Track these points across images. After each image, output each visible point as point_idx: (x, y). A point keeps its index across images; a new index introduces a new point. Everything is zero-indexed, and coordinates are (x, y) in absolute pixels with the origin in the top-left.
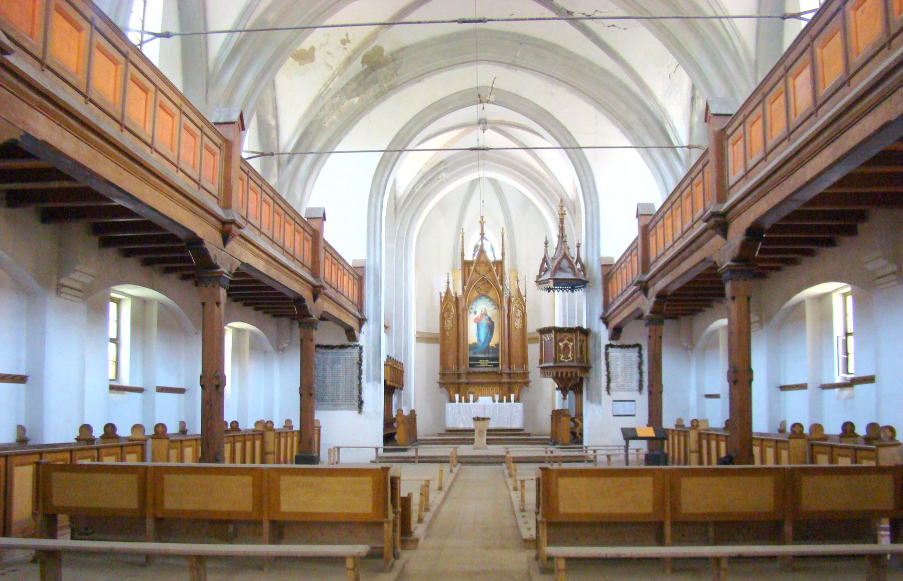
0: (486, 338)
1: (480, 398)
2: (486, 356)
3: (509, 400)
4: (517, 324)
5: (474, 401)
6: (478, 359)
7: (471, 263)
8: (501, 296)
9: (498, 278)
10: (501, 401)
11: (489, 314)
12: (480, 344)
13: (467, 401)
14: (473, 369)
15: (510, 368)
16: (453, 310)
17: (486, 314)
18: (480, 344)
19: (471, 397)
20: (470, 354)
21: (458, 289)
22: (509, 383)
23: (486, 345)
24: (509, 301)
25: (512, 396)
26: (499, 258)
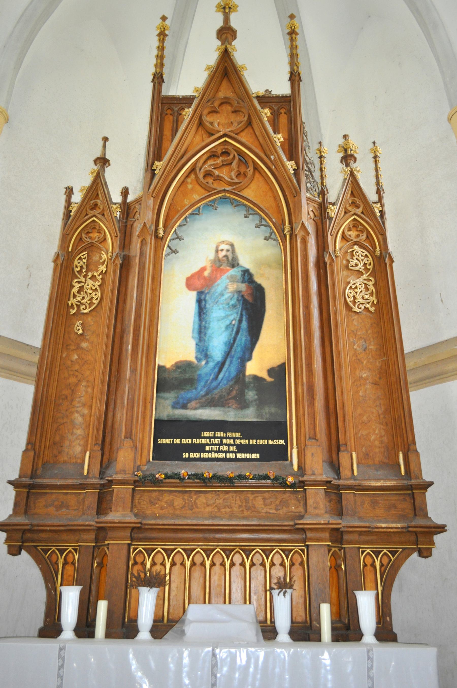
0: (231, 346)
1: (194, 611)
2: (231, 415)
3: (347, 630)
4: (357, 291)
5: (160, 629)
6: (196, 427)
7: (187, 101)
8: (292, 194)
9: (279, 138)
10: (304, 632)
11: (246, 261)
12: (206, 369)
13: (123, 627)
14: (171, 467)
15: (335, 467)
16: (109, 251)
17: (234, 263)
18: (206, 369)
19: (147, 603)
20: (167, 409)
21: (126, 176)
22: (337, 536)
23: (231, 369)
24: (322, 207)
25: (366, 604)
26: (282, 88)
